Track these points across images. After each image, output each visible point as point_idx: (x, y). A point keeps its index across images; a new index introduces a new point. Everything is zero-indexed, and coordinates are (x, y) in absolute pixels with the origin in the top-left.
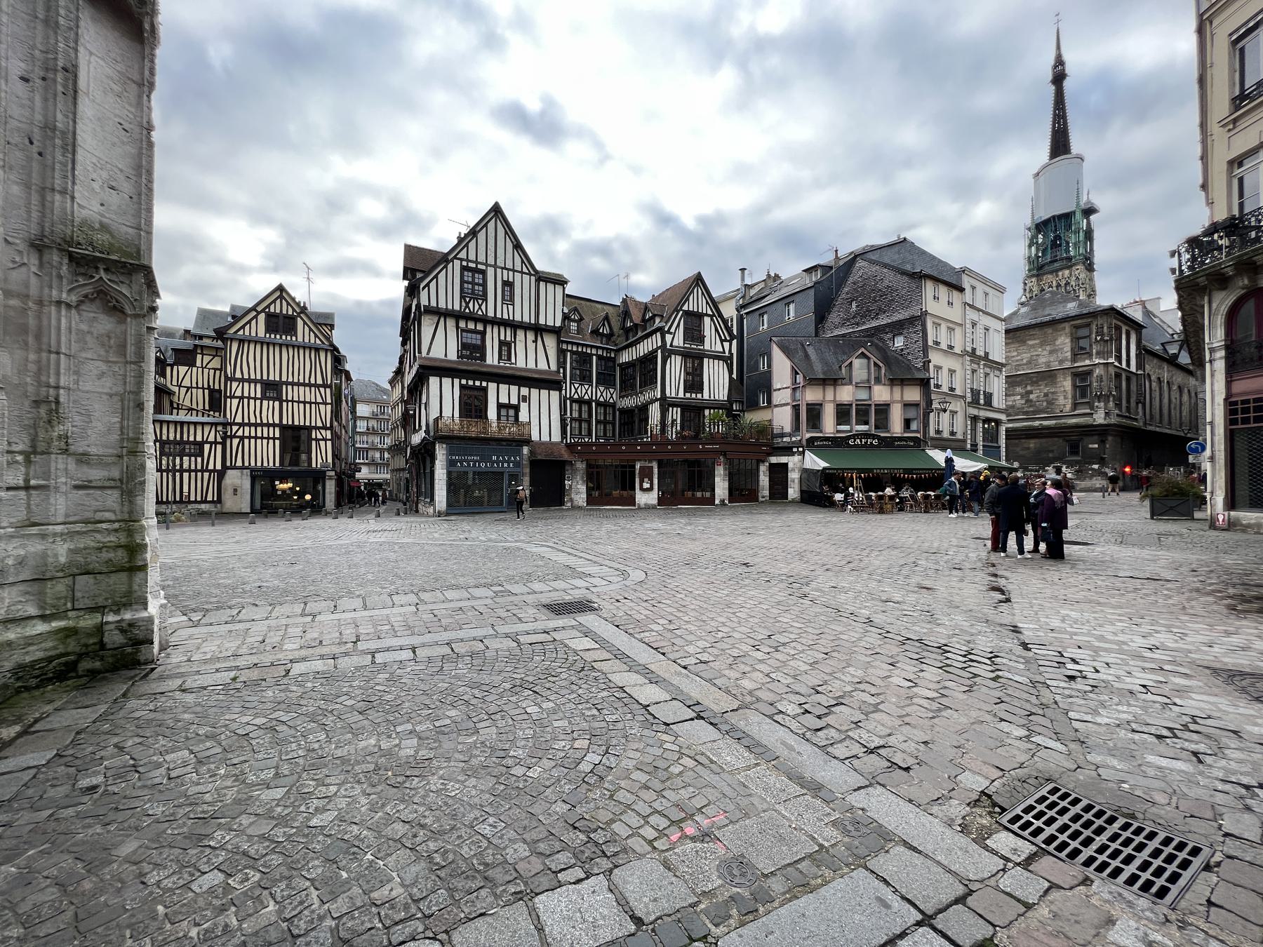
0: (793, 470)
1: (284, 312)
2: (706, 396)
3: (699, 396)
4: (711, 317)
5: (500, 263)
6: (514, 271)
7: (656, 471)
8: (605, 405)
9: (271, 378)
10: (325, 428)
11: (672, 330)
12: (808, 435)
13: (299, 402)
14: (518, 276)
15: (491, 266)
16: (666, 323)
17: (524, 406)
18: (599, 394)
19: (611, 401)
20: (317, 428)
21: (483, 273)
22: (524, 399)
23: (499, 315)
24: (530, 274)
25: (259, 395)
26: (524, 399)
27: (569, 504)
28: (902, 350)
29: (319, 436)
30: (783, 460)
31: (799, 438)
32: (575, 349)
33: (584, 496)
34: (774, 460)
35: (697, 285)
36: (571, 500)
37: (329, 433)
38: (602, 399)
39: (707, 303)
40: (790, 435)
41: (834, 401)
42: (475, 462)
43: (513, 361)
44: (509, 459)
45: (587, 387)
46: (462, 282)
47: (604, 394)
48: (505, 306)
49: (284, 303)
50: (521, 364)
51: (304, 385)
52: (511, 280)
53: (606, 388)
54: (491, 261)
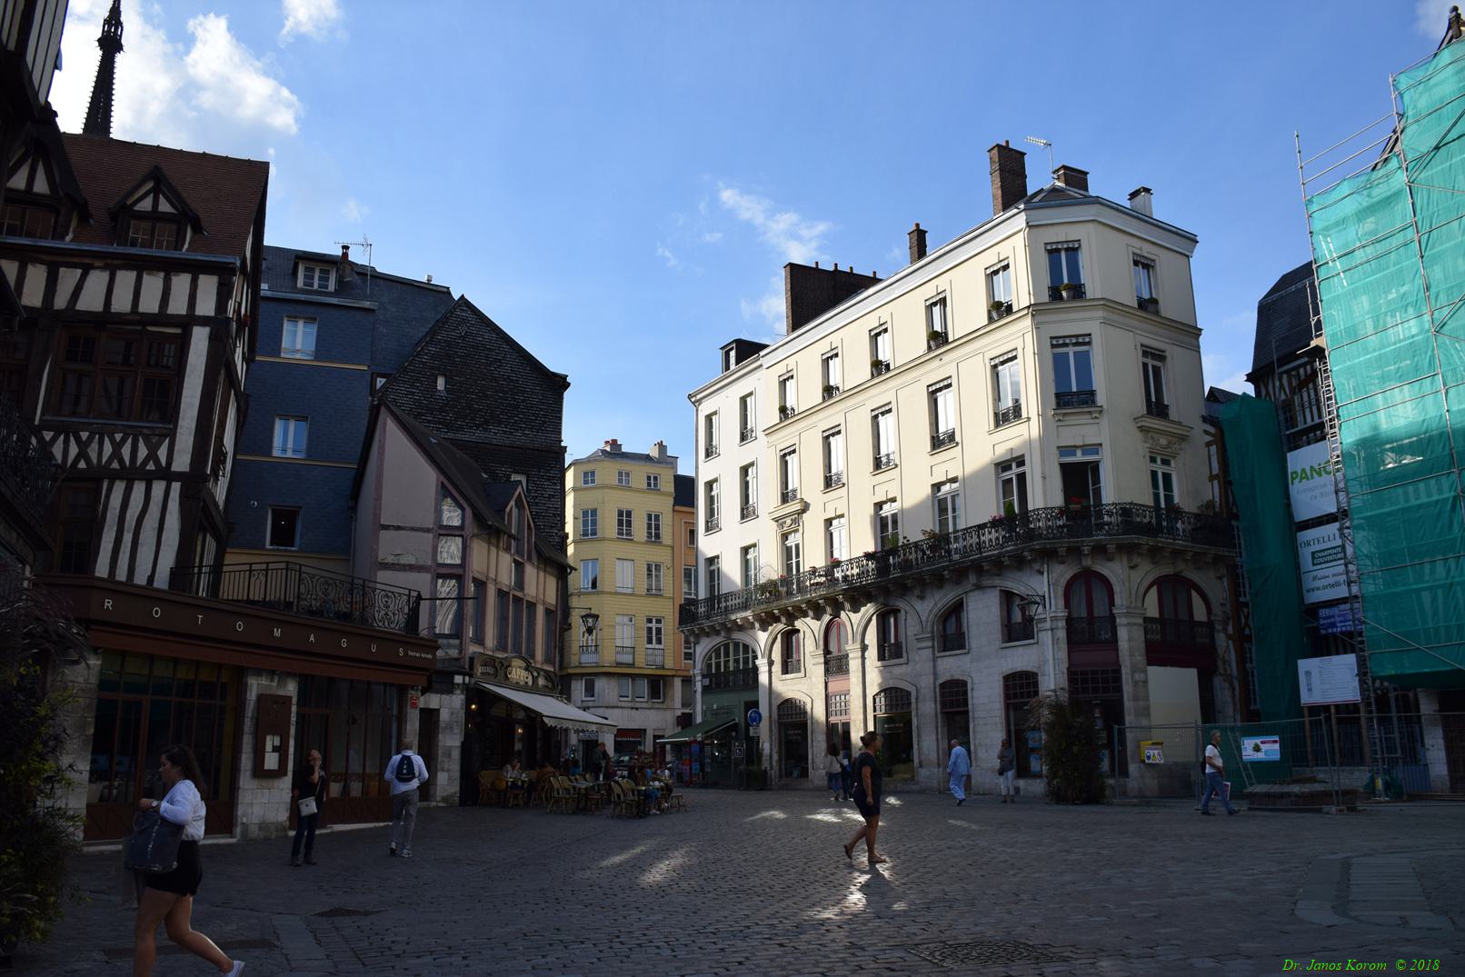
0: (450, 727)
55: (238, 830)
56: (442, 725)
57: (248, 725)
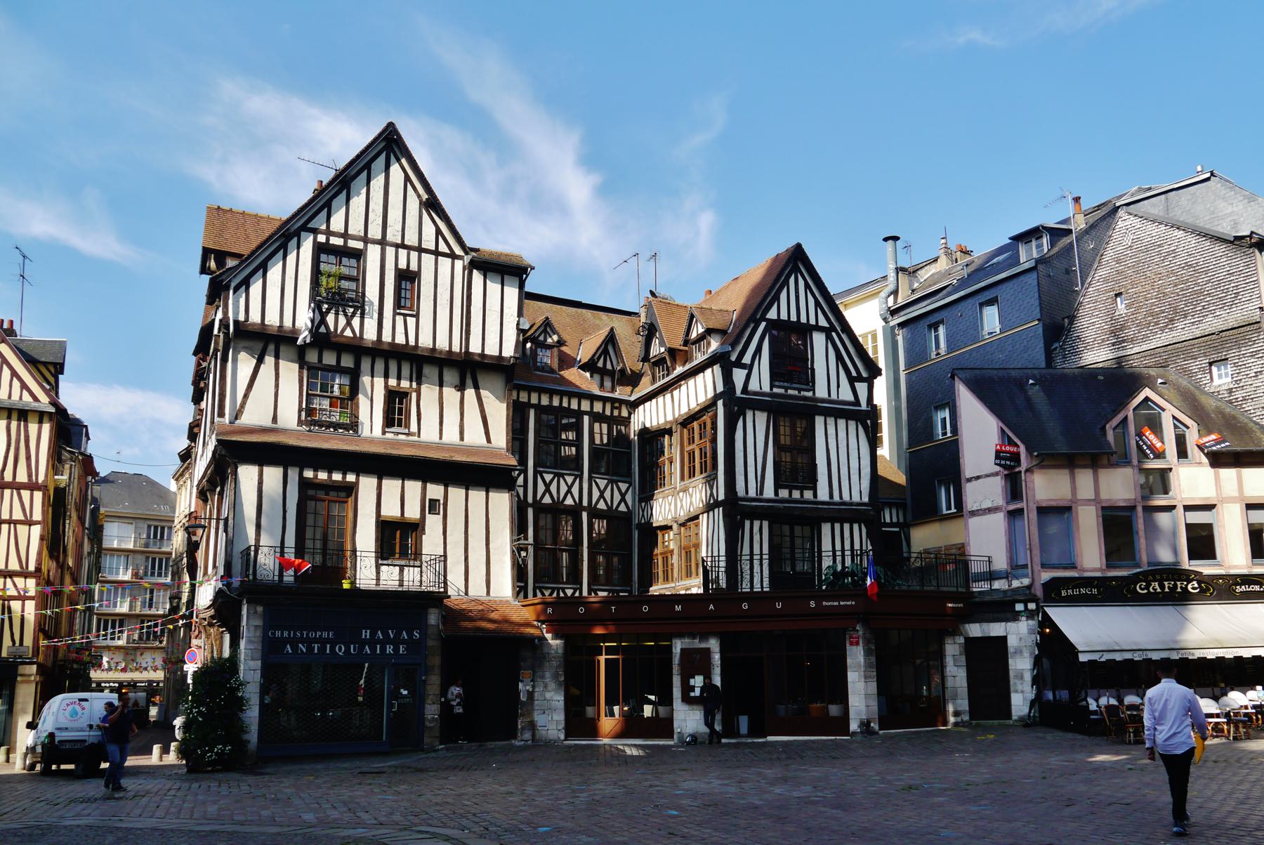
0: (1018, 652)
2: (823, 495)
3: (808, 495)
4: (828, 332)
5: (393, 235)
6: (420, 250)
7: (716, 658)
8: (610, 515)
10: (25, 575)
11: (747, 359)
12: (1046, 576)
14: (428, 259)
15: (375, 242)
16: (734, 345)
17: (433, 523)
18: (596, 494)
19: (623, 508)
21: (358, 255)
22: (433, 506)
23: (387, 337)
24: (453, 256)
26: (433, 506)
27: (527, 735)
28: (1230, 391)
30: (996, 629)
31: (1026, 581)
32: (545, 401)
33: (560, 717)
34: (975, 630)
35: (796, 270)
36: (532, 726)
37: (31, 583)
38: (602, 505)
39: (817, 304)
40: (1006, 576)
41: (1096, 500)
42: (323, 642)
43: (414, 428)
44: (398, 634)
45: (570, 479)
46: (316, 273)
47: (607, 495)
48: (400, 319)
50: (429, 433)
52: (414, 267)
53: (611, 482)
54: (375, 232)
55: (675, 736)
56: (1011, 650)
57: (676, 669)
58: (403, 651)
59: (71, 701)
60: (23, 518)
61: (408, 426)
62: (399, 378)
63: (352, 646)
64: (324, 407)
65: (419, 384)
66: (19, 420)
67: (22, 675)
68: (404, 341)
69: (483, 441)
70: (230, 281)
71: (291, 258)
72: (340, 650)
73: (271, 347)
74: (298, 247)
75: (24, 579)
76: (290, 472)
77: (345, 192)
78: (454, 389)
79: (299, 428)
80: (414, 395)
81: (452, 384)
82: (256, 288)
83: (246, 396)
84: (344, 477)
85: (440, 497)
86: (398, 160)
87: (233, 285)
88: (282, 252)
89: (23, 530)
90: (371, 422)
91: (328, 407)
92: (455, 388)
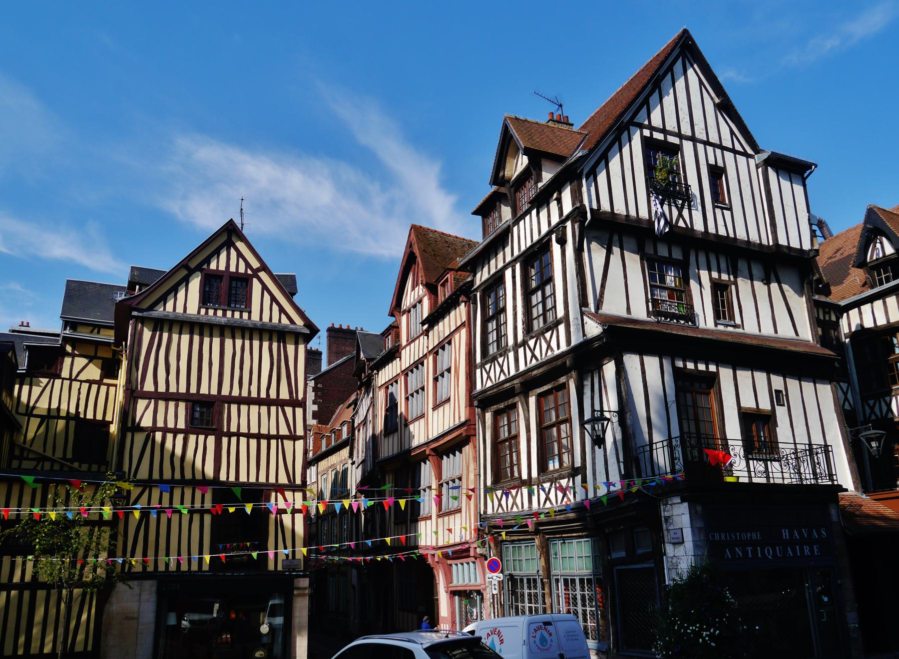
1: (233, 269)
9: (204, 390)
13: (249, 436)
14: (729, 156)
20: (280, 489)
21: (675, 150)
25: (181, 425)
29: (282, 505)
49: (233, 253)
50: (750, 327)
51: (259, 402)
58: (817, 553)
59: (537, 625)
60: (288, 434)
61: (732, 317)
62: (719, 272)
63: (777, 548)
64: (664, 298)
65: (736, 277)
66: (279, 342)
67: (298, 588)
68: (725, 233)
69: (792, 334)
70: (583, 169)
71: (626, 150)
72: (769, 552)
73: (616, 238)
74: (630, 141)
75: (292, 493)
76: (664, 361)
77: (657, 91)
78: (762, 283)
79: (649, 319)
80: (733, 287)
81: (759, 278)
82: (602, 178)
83: (603, 286)
84: (707, 368)
85: (782, 388)
86: (692, 66)
87: (585, 173)
88: (617, 144)
89: (288, 444)
90: (704, 314)
91: (667, 299)
92: (762, 281)
